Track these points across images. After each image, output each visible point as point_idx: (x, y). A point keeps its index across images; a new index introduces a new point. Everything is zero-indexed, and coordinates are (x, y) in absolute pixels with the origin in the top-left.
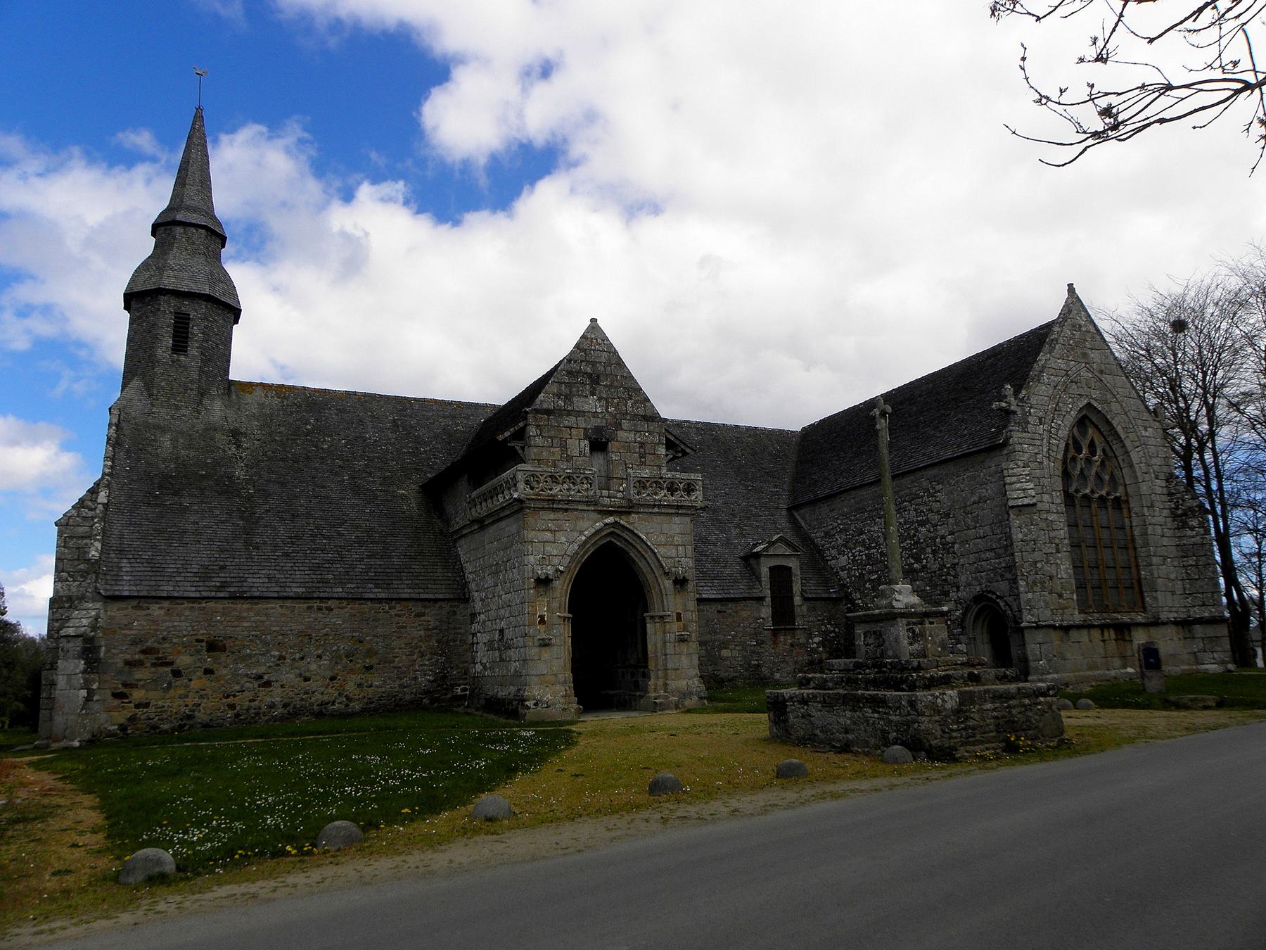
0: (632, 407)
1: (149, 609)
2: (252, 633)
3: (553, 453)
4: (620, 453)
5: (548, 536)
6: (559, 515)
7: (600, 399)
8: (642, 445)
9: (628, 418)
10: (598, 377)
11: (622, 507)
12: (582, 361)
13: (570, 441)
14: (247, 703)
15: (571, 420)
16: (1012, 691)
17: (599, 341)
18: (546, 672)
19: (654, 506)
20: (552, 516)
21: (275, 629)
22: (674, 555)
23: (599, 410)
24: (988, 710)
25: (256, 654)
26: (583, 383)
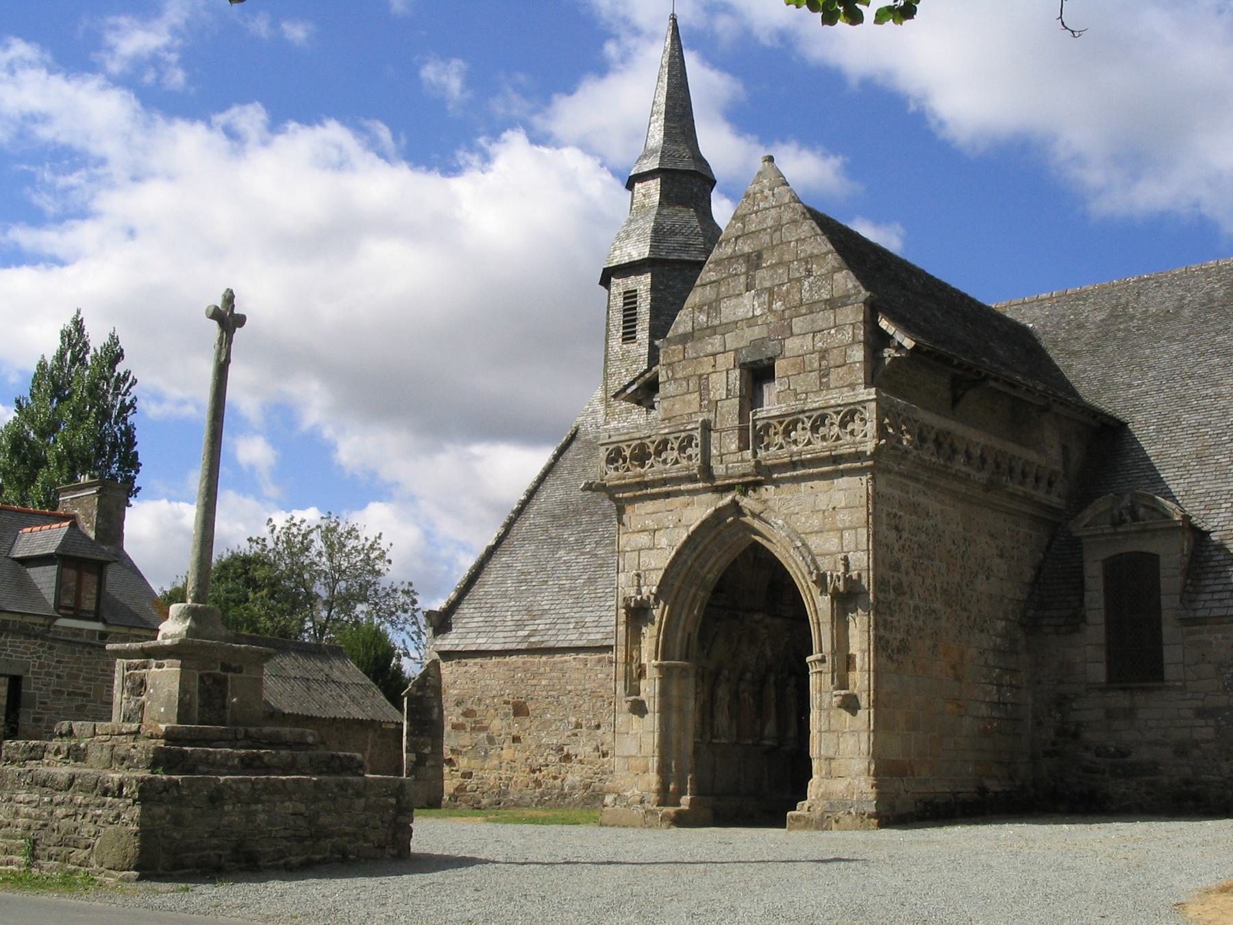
0: (811, 289)
1: (466, 665)
2: (549, 694)
3: (690, 403)
4: (788, 377)
5: (644, 539)
6: (660, 504)
7: (758, 295)
8: (824, 353)
9: (803, 311)
10: (759, 256)
11: (744, 475)
12: (737, 238)
13: (714, 376)
14: (551, 780)
15: (715, 343)
16: (60, 778)
17: (767, 192)
18: (633, 753)
19: (793, 465)
20: (649, 506)
21: (569, 688)
22: (833, 549)
23: (758, 312)
24: (21, 802)
25: (555, 720)
26: (736, 274)
